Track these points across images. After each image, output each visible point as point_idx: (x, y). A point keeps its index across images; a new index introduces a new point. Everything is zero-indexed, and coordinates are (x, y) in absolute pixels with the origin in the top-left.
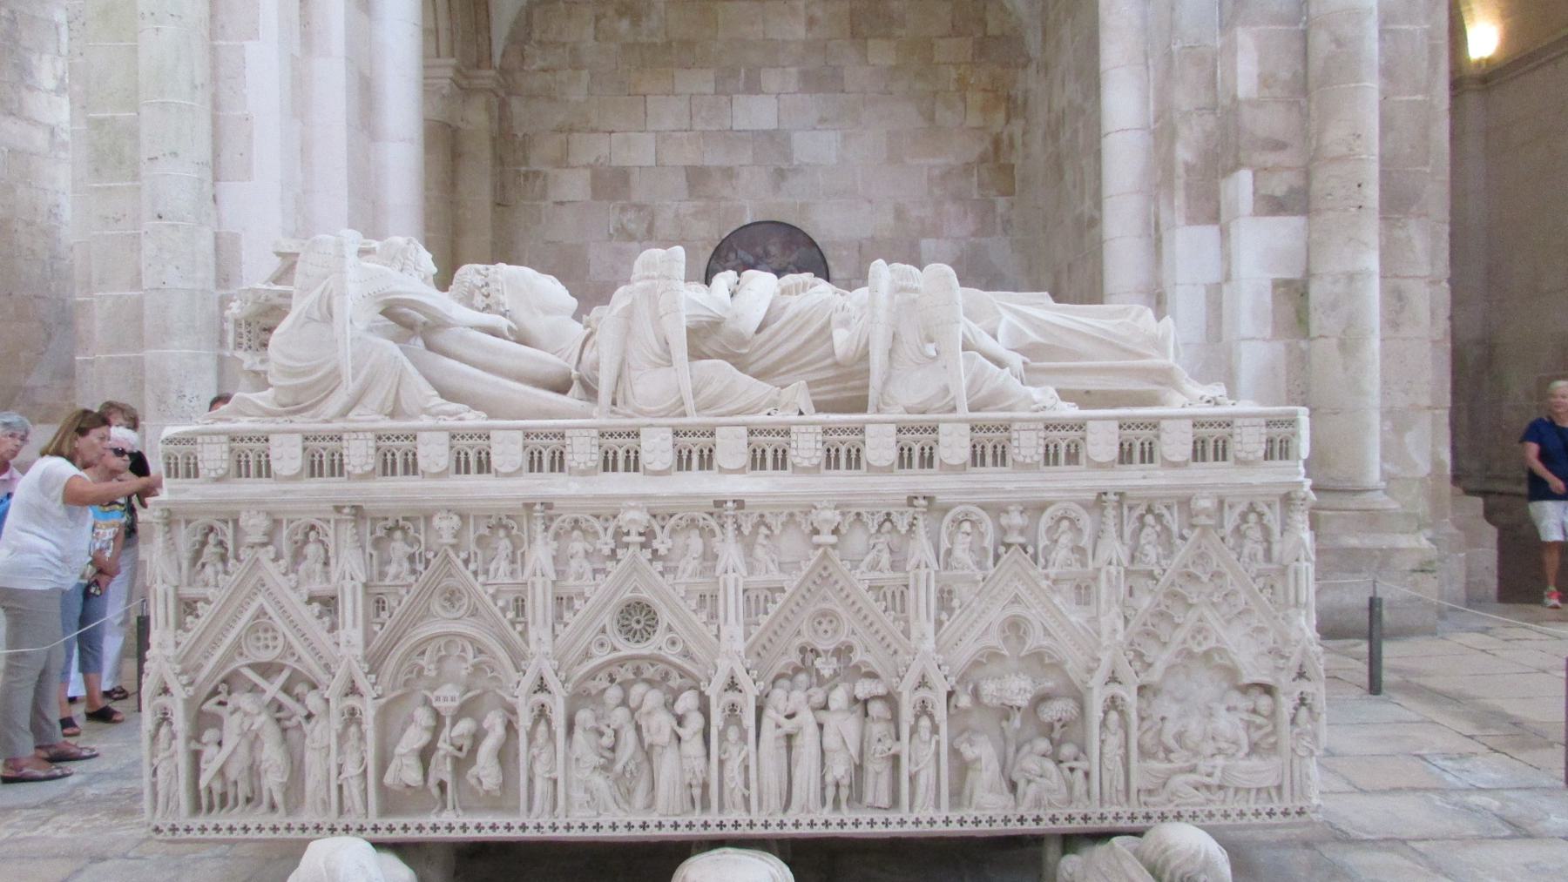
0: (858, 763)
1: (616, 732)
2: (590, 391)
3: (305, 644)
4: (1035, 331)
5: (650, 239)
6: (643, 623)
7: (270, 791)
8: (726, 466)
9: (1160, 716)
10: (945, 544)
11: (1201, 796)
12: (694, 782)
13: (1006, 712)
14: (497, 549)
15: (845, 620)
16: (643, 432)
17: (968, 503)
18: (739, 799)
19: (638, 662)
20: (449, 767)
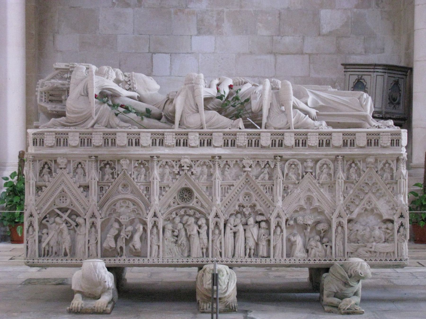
0: (257, 241)
1: (179, 230)
2: (171, 120)
3: (77, 201)
4: (322, 101)
5: (140, 6)
6: (187, 195)
7: (65, 249)
8: (216, 145)
9: (356, 230)
10: (286, 171)
11: (368, 255)
12: (204, 247)
13: (305, 226)
14: (140, 171)
15: (253, 196)
16: (189, 133)
17: (293, 158)
18: (219, 253)
19: (185, 209)
20: (124, 242)
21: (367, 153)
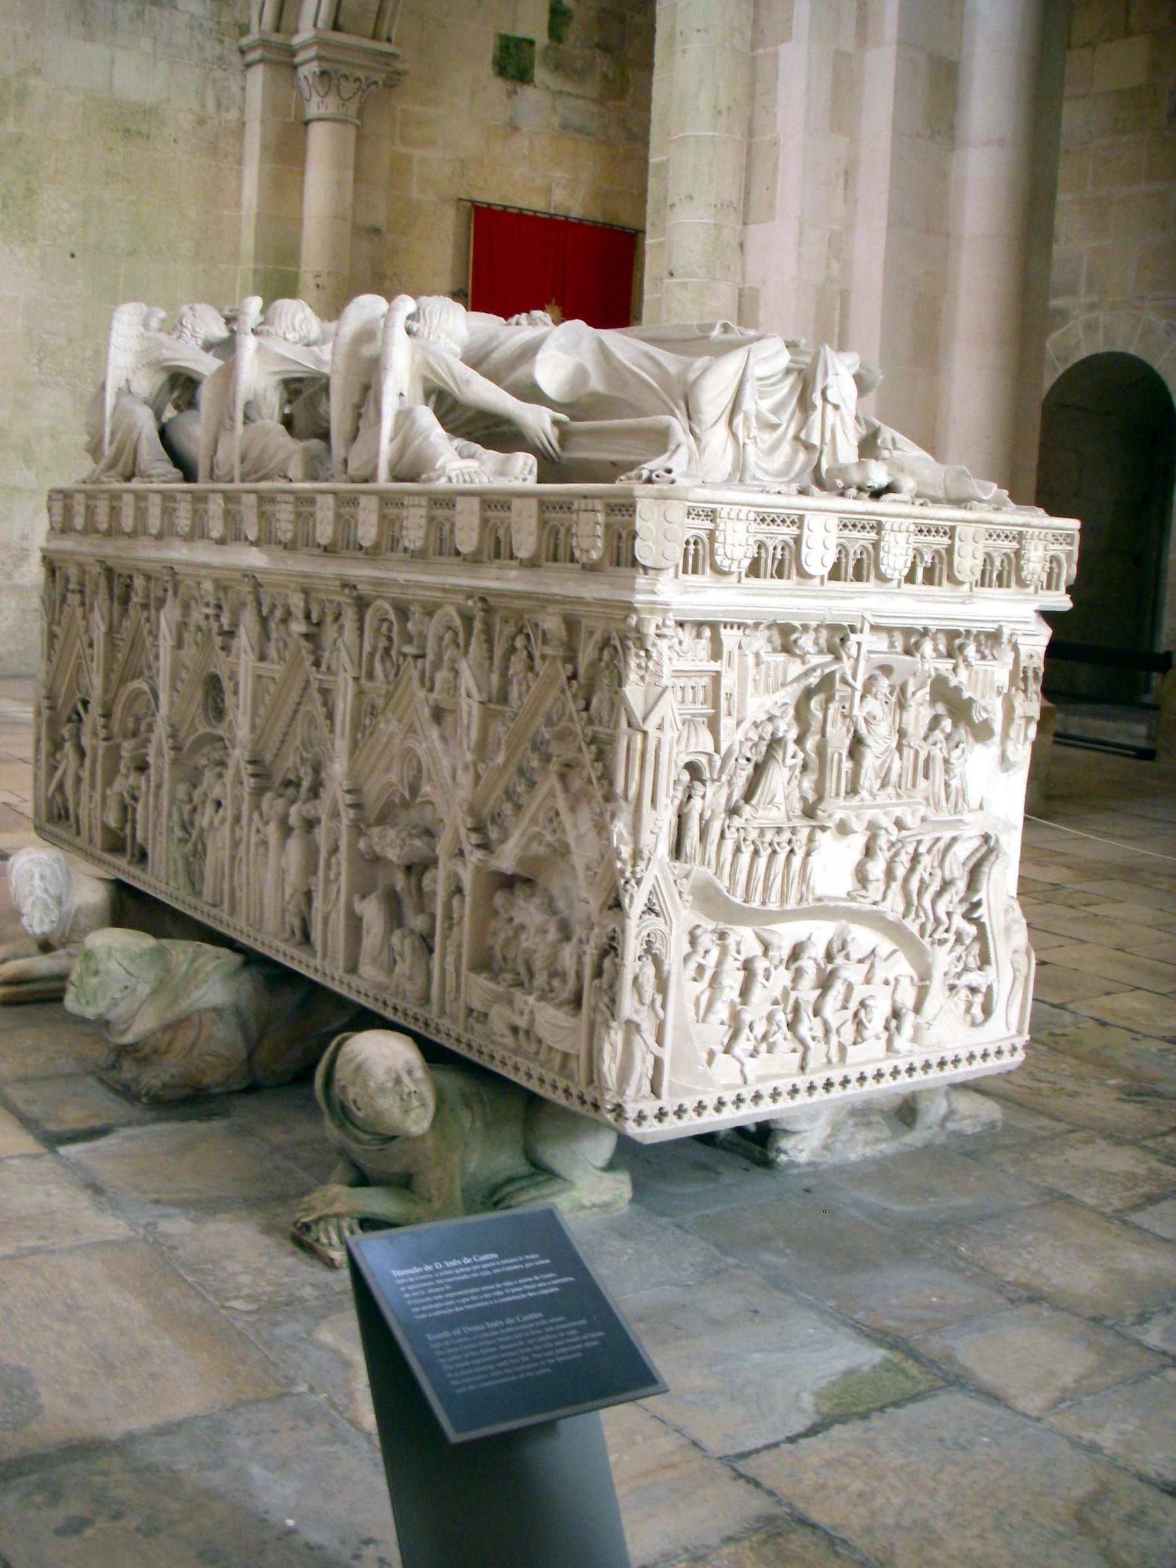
10: (367, 648)
11: (509, 1040)
21: (542, 589)
